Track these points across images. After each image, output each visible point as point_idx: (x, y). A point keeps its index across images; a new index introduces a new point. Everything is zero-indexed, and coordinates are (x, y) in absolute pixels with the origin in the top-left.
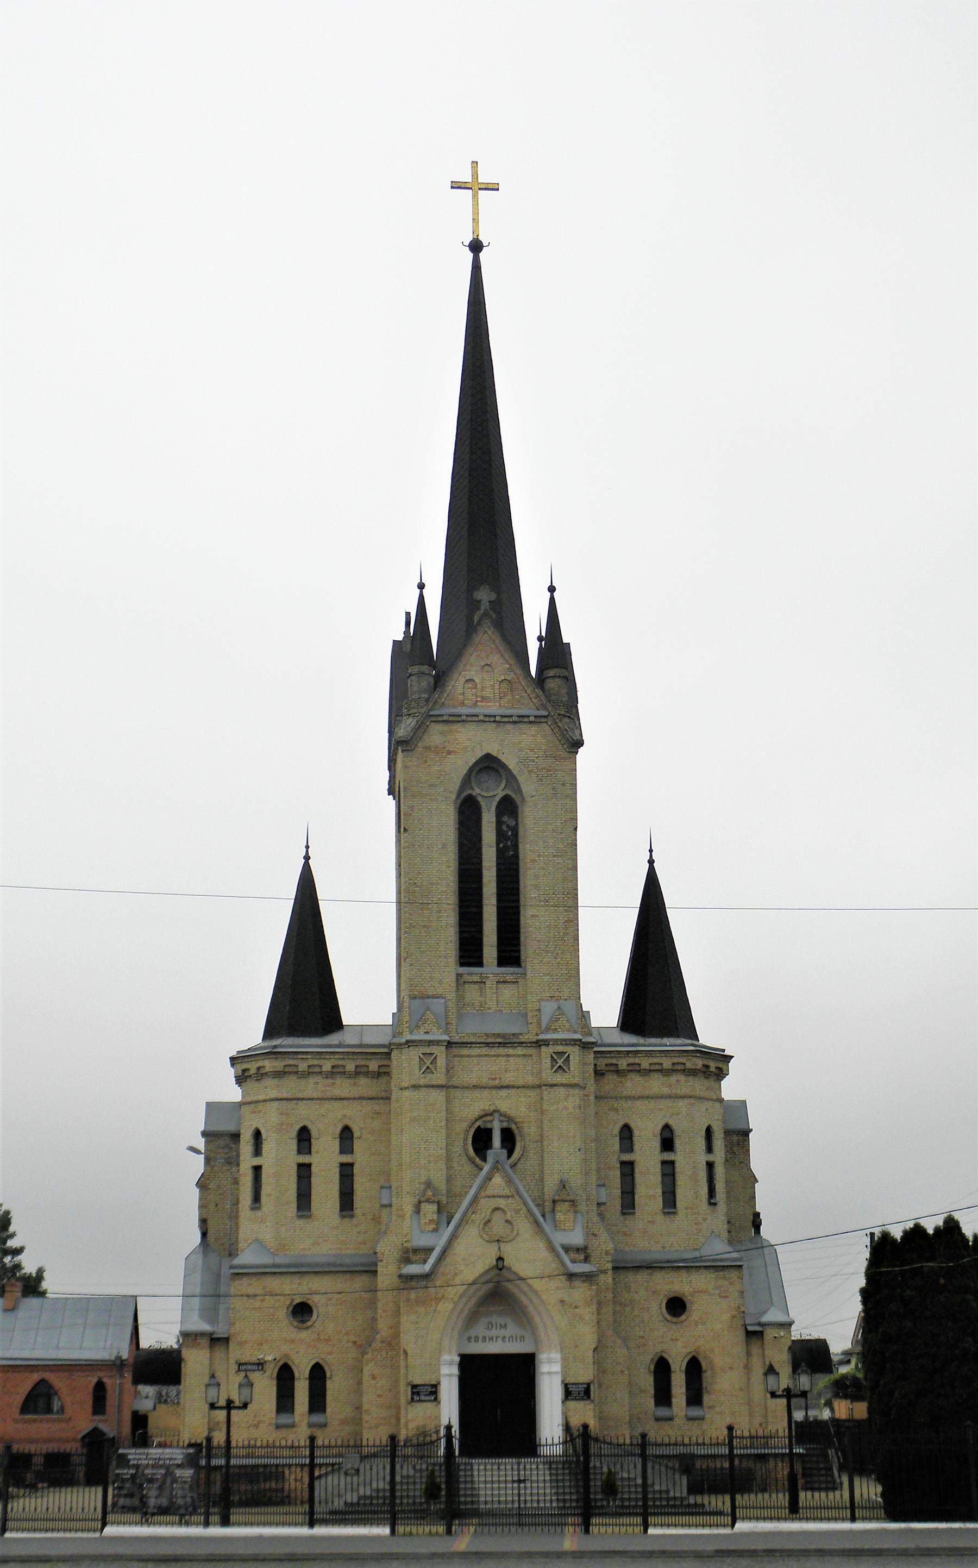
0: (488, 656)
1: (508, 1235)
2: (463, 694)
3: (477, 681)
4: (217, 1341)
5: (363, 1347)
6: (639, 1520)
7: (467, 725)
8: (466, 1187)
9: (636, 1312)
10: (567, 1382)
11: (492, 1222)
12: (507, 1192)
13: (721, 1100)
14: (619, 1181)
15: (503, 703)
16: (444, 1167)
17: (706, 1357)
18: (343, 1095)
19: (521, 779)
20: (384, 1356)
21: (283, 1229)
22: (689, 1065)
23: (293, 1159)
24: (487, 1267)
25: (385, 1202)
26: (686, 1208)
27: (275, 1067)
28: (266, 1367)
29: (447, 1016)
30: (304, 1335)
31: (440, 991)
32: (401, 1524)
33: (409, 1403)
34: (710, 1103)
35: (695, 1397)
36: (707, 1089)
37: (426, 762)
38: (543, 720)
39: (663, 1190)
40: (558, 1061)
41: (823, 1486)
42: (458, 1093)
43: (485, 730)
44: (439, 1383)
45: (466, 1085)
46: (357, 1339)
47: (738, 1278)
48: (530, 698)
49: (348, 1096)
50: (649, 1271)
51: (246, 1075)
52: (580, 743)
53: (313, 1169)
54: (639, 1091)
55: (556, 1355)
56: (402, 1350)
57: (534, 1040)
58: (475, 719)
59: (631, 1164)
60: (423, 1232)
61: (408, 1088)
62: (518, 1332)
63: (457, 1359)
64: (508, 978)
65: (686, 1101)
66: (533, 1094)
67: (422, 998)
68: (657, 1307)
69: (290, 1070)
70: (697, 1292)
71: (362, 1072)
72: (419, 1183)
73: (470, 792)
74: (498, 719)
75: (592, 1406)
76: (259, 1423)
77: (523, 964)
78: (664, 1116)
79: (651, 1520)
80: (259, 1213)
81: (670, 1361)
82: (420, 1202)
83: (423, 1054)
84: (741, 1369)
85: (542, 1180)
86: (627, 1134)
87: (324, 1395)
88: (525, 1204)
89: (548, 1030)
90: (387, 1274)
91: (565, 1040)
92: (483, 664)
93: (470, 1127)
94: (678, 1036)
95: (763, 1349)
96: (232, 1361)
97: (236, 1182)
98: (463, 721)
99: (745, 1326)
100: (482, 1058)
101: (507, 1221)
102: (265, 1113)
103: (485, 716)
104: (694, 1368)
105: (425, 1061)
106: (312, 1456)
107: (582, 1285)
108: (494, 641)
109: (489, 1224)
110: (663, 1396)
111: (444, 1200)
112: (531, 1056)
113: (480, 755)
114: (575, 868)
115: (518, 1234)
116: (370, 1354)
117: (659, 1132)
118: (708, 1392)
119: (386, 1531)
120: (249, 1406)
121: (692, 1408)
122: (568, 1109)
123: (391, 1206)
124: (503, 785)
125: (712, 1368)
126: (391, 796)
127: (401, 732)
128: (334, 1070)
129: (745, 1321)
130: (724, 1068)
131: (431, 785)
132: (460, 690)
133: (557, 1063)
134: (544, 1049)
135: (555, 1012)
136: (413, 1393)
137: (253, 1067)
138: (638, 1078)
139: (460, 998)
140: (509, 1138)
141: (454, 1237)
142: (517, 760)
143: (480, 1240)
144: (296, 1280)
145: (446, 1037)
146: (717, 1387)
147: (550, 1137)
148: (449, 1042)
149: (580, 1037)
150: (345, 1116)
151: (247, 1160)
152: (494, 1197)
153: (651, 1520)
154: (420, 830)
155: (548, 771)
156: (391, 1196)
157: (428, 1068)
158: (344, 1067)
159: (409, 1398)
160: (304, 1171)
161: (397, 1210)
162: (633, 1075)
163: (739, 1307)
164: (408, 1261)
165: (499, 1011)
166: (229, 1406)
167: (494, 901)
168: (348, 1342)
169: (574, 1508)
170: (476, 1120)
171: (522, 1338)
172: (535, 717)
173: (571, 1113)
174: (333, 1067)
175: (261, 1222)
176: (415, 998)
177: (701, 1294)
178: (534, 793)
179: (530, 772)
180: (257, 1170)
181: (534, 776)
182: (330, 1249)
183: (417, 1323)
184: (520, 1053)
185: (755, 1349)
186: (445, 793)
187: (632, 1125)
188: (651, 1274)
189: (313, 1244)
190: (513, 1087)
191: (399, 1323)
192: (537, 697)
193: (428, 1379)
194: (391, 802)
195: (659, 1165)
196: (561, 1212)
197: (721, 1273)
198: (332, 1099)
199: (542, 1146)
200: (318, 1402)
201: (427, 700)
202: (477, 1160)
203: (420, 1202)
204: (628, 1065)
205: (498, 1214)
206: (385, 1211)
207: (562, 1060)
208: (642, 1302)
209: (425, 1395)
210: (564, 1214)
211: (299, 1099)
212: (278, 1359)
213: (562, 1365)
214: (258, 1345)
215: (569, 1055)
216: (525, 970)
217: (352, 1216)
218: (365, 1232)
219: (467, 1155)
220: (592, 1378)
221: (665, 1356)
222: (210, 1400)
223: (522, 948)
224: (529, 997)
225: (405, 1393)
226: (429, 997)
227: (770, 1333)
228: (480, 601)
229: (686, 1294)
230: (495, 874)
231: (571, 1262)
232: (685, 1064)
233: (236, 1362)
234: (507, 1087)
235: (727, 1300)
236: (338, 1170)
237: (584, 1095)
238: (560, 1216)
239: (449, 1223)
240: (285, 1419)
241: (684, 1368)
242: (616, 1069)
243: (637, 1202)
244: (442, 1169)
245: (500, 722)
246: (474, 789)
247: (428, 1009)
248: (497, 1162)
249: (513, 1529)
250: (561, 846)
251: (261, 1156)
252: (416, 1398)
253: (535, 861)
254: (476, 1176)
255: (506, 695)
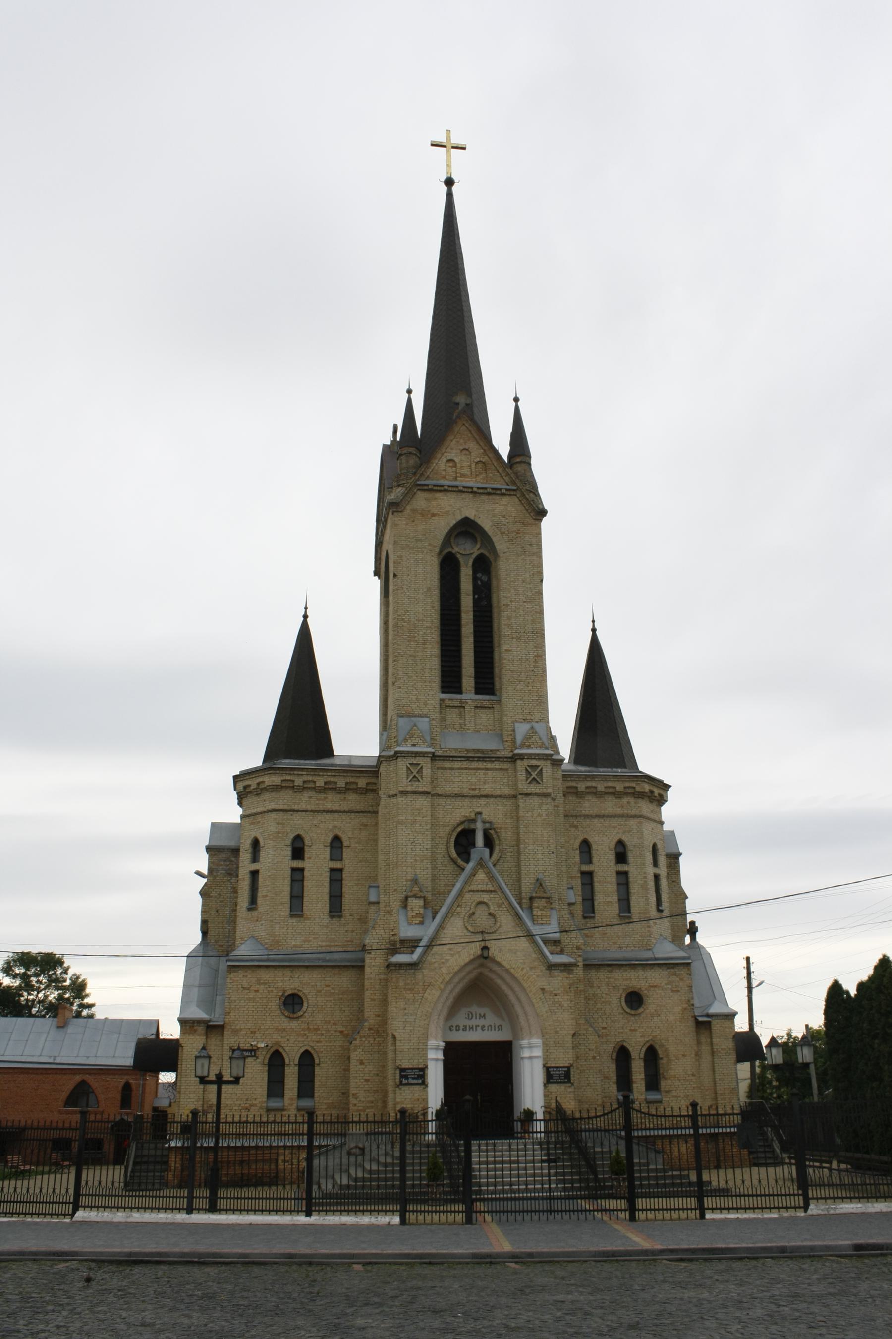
0: (465, 443)
1: (491, 927)
2: (445, 470)
3: (457, 460)
4: (212, 1029)
5: (349, 1037)
6: (692, 1202)
7: (449, 494)
8: (449, 886)
9: (599, 1006)
10: (549, 1065)
11: (477, 915)
12: (490, 887)
13: (662, 823)
14: (580, 888)
15: (478, 479)
16: (429, 866)
17: (662, 1046)
18: (334, 809)
19: (494, 539)
20: (372, 1042)
21: (277, 927)
22: (638, 789)
23: (288, 863)
24: (472, 957)
25: (373, 898)
26: (640, 913)
27: (273, 781)
28: (257, 1053)
29: (431, 733)
30: (294, 1024)
31: (425, 711)
32: (413, 1211)
33: (398, 1086)
34: (655, 824)
35: (653, 1083)
36: (652, 812)
37: (413, 521)
38: (512, 493)
39: (618, 896)
40: (532, 773)
41: (771, 1161)
42: (442, 801)
43: (463, 499)
44: (427, 1067)
45: (449, 793)
46: (344, 1029)
47: (687, 974)
48: (502, 476)
49: (338, 808)
50: (610, 968)
51: (247, 790)
52: (543, 513)
53: (306, 873)
54: (595, 811)
55: (537, 1041)
56: (390, 1035)
57: (510, 755)
58: (455, 489)
59: (590, 874)
60: (410, 924)
61: (396, 795)
62: (498, 1021)
63: (443, 1044)
64: (486, 704)
65: (636, 820)
66: (509, 803)
67: (409, 716)
68: (616, 1001)
69: (287, 785)
70: (652, 987)
71: (351, 789)
72: (407, 880)
73: (450, 550)
74: (475, 489)
75: (571, 1089)
76: (251, 1106)
77: (497, 693)
78: (618, 833)
79: (708, 1202)
80: (255, 913)
81: (631, 1050)
82: (407, 898)
83: (410, 764)
84: (693, 1056)
85: (519, 880)
86: (586, 847)
87: (313, 1081)
88: (507, 898)
89: (523, 746)
90: (374, 964)
91: (538, 755)
92: (461, 448)
93: (453, 831)
94: (626, 768)
95: (711, 1038)
96: (226, 1047)
97: (235, 891)
98: (445, 491)
99: (695, 1017)
100: (462, 771)
101: (490, 914)
102: (264, 823)
103: (464, 487)
104: (652, 1055)
105: (413, 770)
106: (311, 1135)
107: (560, 974)
108: (470, 431)
109: (473, 917)
110: (624, 1081)
111: (429, 896)
112: (507, 769)
113: (459, 518)
114: (541, 612)
115: (500, 927)
116: (358, 1040)
117: (614, 846)
118: (666, 1079)
119: (396, 1220)
120: (241, 1081)
121: (650, 1093)
122: (541, 816)
123: (378, 903)
124: (478, 546)
125: (667, 1056)
126: (377, 577)
127: (391, 497)
128: (327, 786)
129: (694, 1012)
130: (664, 794)
131: (417, 540)
132: (442, 467)
133: (531, 775)
134: (519, 762)
135: (529, 730)
136: (401, 1076)
137: (253, 783)
138: (594, 800)
139: (443, 719)
140: (489, 842)
141: (441, 927)
142: (491, 523)
143: (465, 931)
144: (288, 973)
145: (430, 750)
146: (672, 1073)
147: (527, 841)
148: (433, 754)
149: (549, 752)
150: (335, 827)
151: (245, 865)
152: (478, 891)
153: (708, 1202)
154: (408, 575)
155: (517, 533)
156: (379, 896)
157: (415, 776)
158: (336, 783)
159: (398, 1080)
160: (297, 876)
161: (385, 906)
162: (589, 797)
163: (689, 1001)
164: (394, 951)
165: (477, 731)
166: (219, 1080)
167: (471, 639)
168: (336, 1031)
169: (580, 1189)
170: (459, 825)
171: (500, 1027)
172: (507, 490)
173: (544, 820)
174: (326, 783)
175: (257, 921)
176: (402, 716)
177: (656, 989)
178: (506, 551)
179: (502, 533)
180: (255, 874)
181: (506, 537)
182: (321, 946)
183: (405, 1009)
184: (497, 767)
185: (704, 1039)
186: (430, 547)
187: (591, 840)
188: (611, 971)
189: (305, 942)
190: (492, 797)
191: (386, 1011)
192: (508, 474)
193: (416, 1063)
194: (376, 583)
195: (615, 874)
196: (538, 907)
197: (672, 970)
198: (324, 811)
199: (519, 849)
200: (306, 1087)
201: (415, 474)
202: (460, 862)
203: (407, 898)
204: (587, 787)
205: (482, 908)
206: (373, 908)
207: (536, 773)
208: (604, 995)
209: (413, 1078)
210: (541, 910)
211: (294, 811)
212: (270, 1045)
213: (543, 1050)
214: (252, 1032)
215: (541, 770)
216: (501, 696)
217: (340, 917)
218: (353, 931)
219: (450, 857)
220: (571, 1062)
221: (625, 1044)
222: (199, 1073)
223: (496, 679)
224: (505, 718)
225: (392, 1076)
226: (415, 716)
227: (716, 1025)
228: (458, 404)
229: (643, 989)
230: (472, 617)
231: (552, 953)
232: (634, 788)
233: (231, 1048)
234: (486, 796)
235: (679, 994)
236: (328, 874)
237: (555, 806)
238: (537, 912)
239: (434, 918)
240: (274, 1103)
241: (642, 1056)
242: (575, 791)
243: (596, 907)
244: (427, 868)
245: (475, 493)
246: (453, 548)
247: (415, 725)
248: (481, 859)
249: (544, 1217)
250: (530, 594)
251: (258, 861)
252: (404, 1081)
253: (508, 605)
254: (458, 876)
255: (481, 473)
